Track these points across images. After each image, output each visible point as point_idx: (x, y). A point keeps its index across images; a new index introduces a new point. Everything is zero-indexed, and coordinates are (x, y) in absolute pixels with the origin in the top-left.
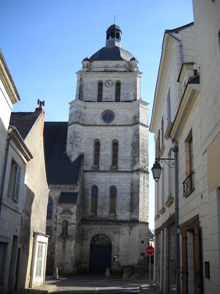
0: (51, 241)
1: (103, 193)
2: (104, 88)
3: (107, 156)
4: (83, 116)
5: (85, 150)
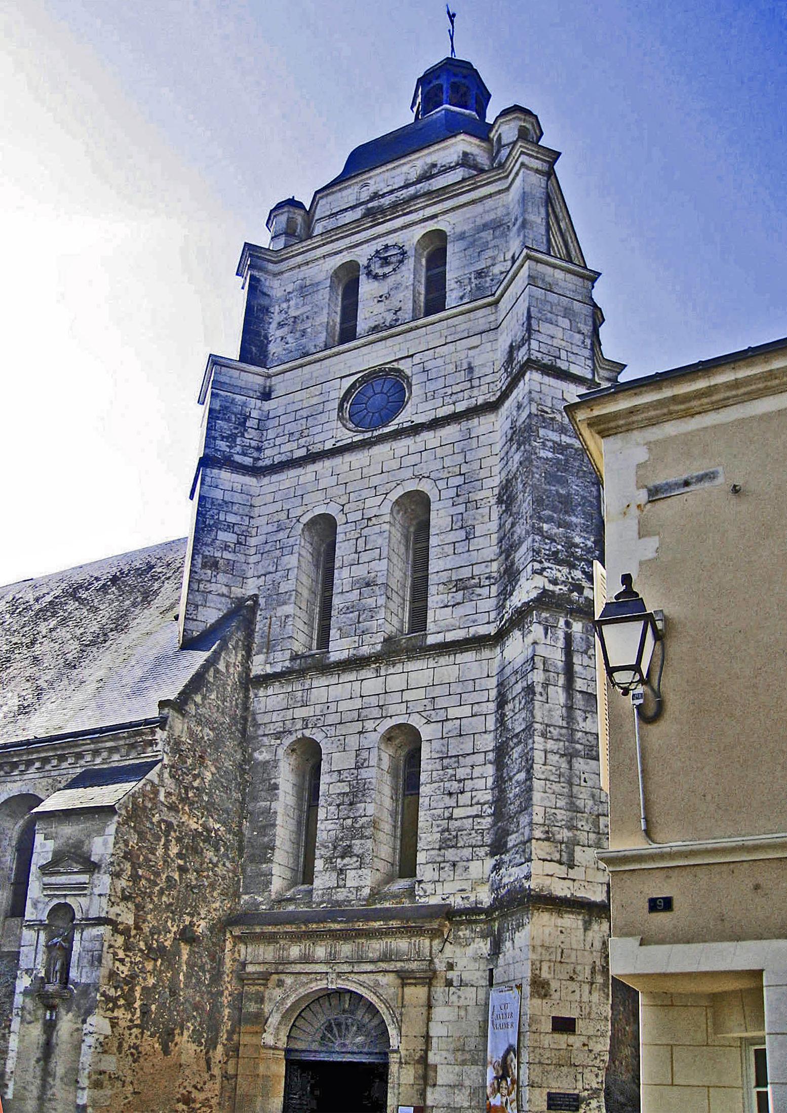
3: (368, 585)
4: (251, 433)
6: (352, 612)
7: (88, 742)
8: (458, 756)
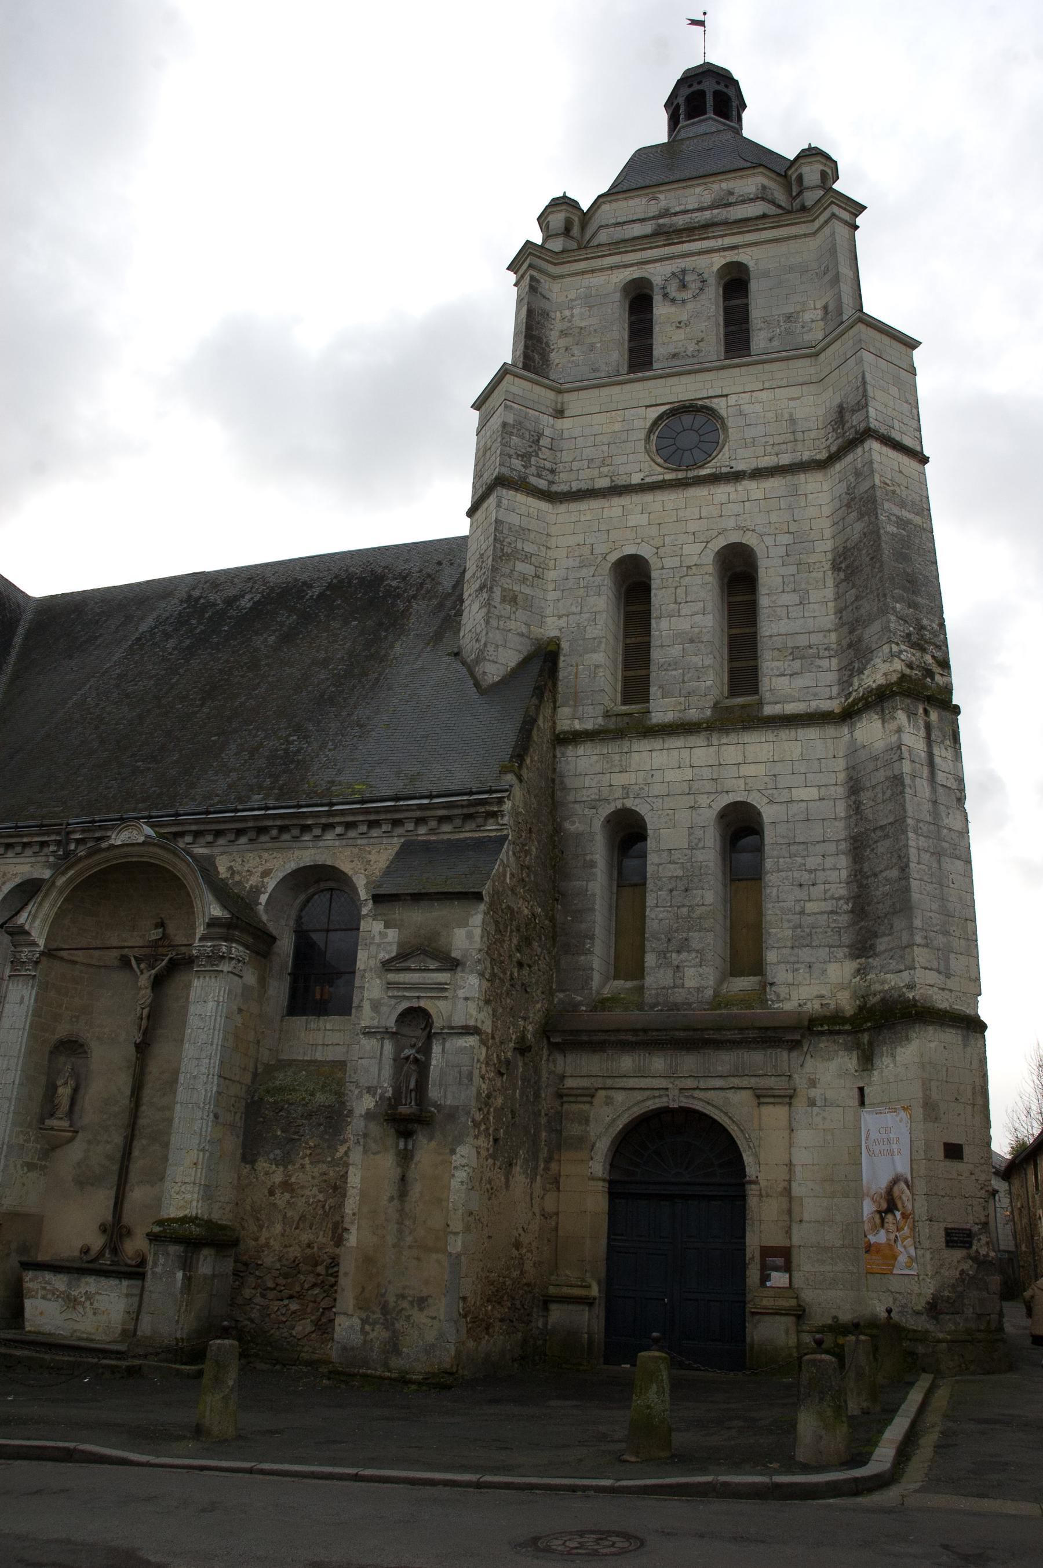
0: (338, 1155)
1: (676, 855)
2: (661, 310)
3: (692, 641)
4: (545, 453)
5: (562, 622)
6: (675, 669)
7: (415, 807)
8: (807, 843)
